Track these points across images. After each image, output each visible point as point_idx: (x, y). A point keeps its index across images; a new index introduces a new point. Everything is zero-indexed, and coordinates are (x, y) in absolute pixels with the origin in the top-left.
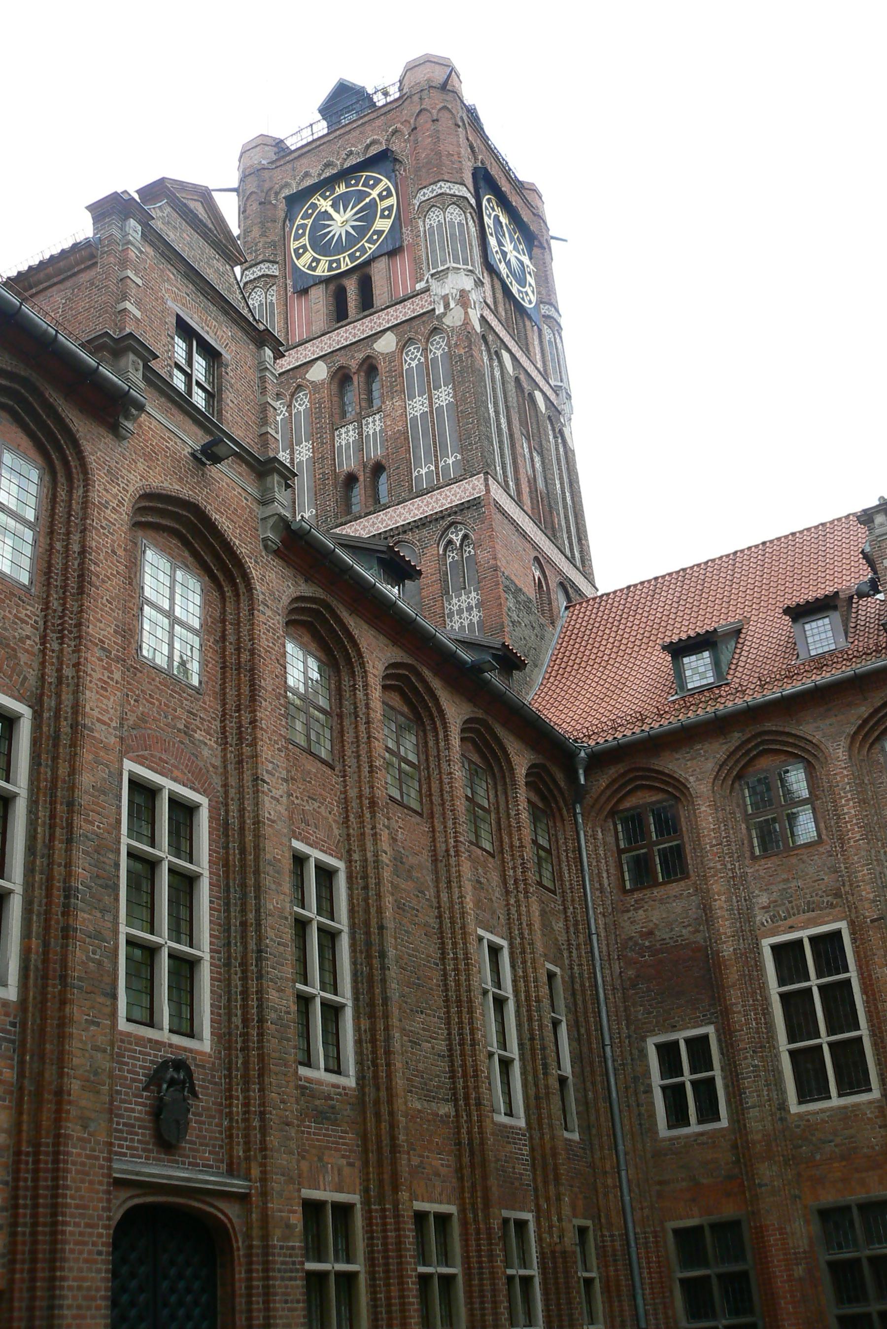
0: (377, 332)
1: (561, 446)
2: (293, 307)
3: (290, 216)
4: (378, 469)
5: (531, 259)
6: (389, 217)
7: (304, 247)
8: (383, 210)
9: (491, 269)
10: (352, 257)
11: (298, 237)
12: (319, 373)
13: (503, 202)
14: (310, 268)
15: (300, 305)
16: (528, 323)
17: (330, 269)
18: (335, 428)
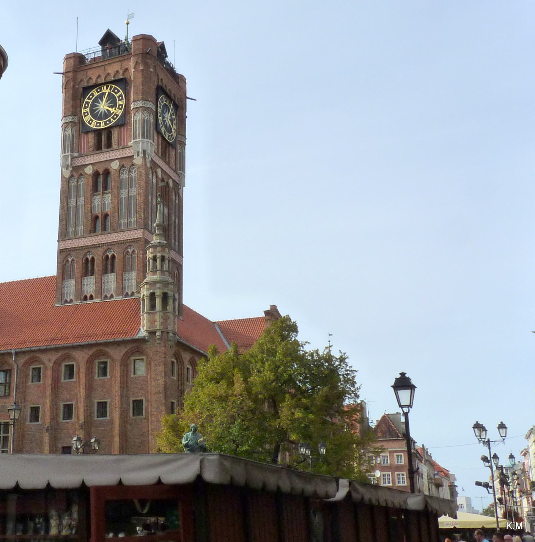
0: (111, 157)
1: (177, 199)
2: (81, 137)
3: (84, 96)
4: (107, 215)
5: (176, 115)
6: (121, 109)
7: (87, 112)
8: (119, 105)
9: (159, 132)
10: (106, 124)
11: (85, 108)
12: (89, 170)
13: (168, 96)
14: (89, 122)
15: (84, 137)
16: (171, 148)
17: (97, 126)
18: (93, 195)
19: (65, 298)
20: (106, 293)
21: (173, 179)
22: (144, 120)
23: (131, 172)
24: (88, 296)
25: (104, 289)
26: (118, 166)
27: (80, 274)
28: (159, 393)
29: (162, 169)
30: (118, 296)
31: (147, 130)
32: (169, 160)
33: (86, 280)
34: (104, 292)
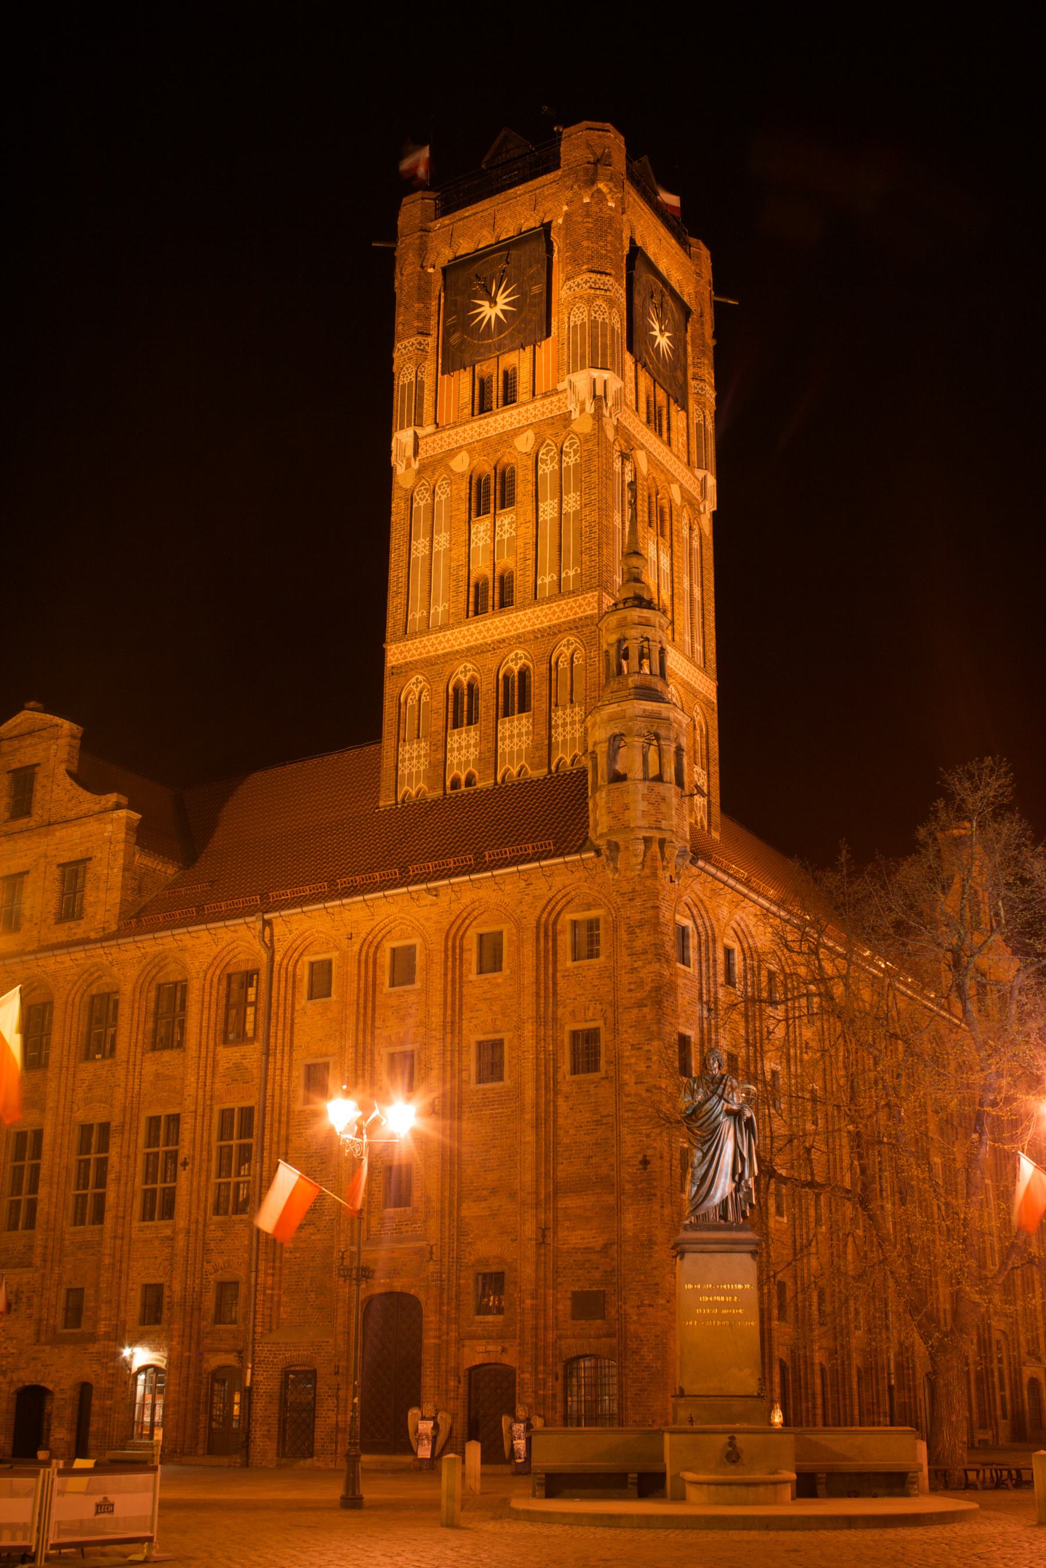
12: (461, 464)
19: (406, 788)
20: (508, 766)
21: (681, 486)
22: (594, 323)
23: (567, 454)
24: (463, 777)
25: (504, 753)
26: (531, 442)
27: (441, 723)
28: (641, 1005)
29: (649, 454)
30: (537, 769)
31: (604, 345)
32: (669, 438)
33: (456, 737)
34: (504, 762)
